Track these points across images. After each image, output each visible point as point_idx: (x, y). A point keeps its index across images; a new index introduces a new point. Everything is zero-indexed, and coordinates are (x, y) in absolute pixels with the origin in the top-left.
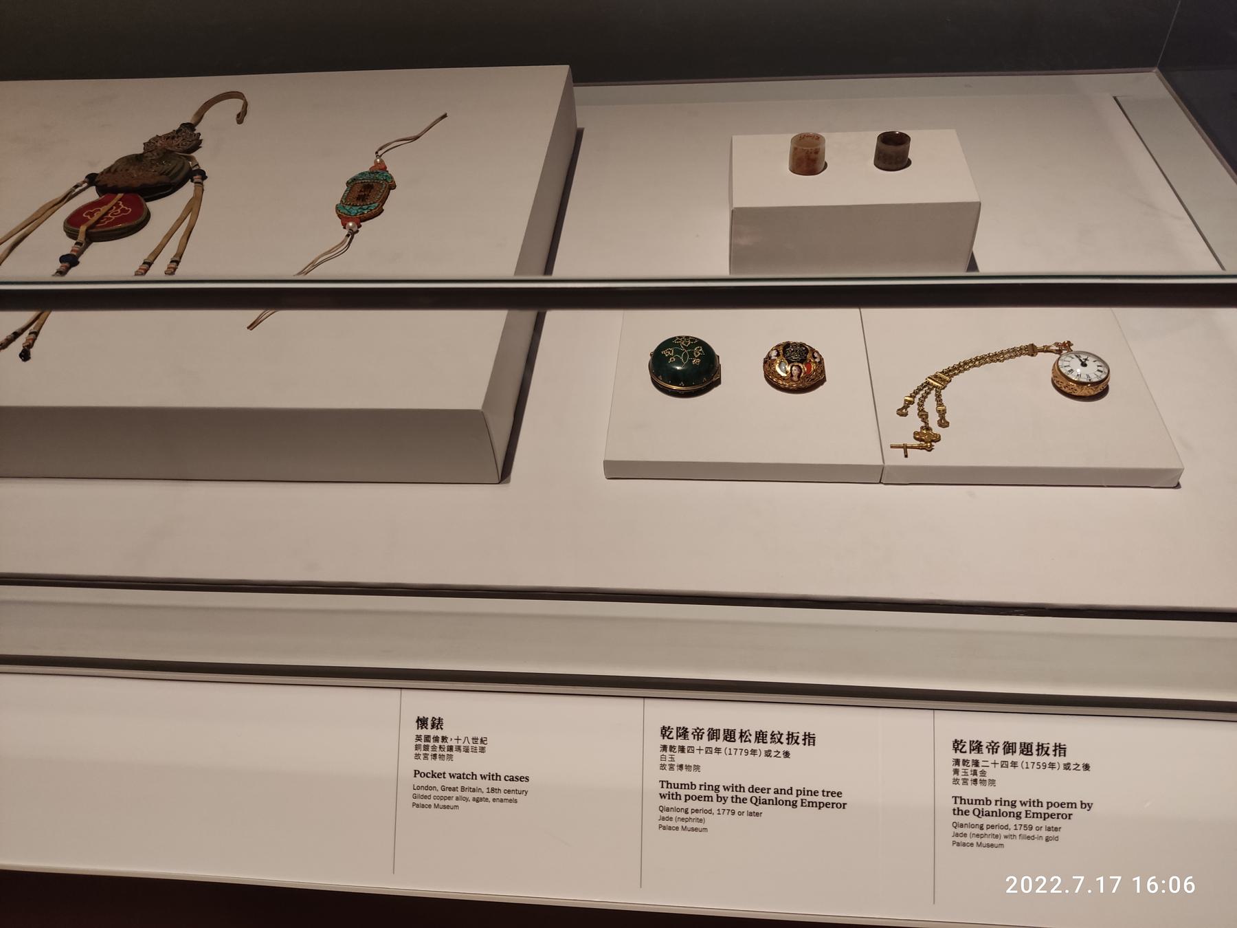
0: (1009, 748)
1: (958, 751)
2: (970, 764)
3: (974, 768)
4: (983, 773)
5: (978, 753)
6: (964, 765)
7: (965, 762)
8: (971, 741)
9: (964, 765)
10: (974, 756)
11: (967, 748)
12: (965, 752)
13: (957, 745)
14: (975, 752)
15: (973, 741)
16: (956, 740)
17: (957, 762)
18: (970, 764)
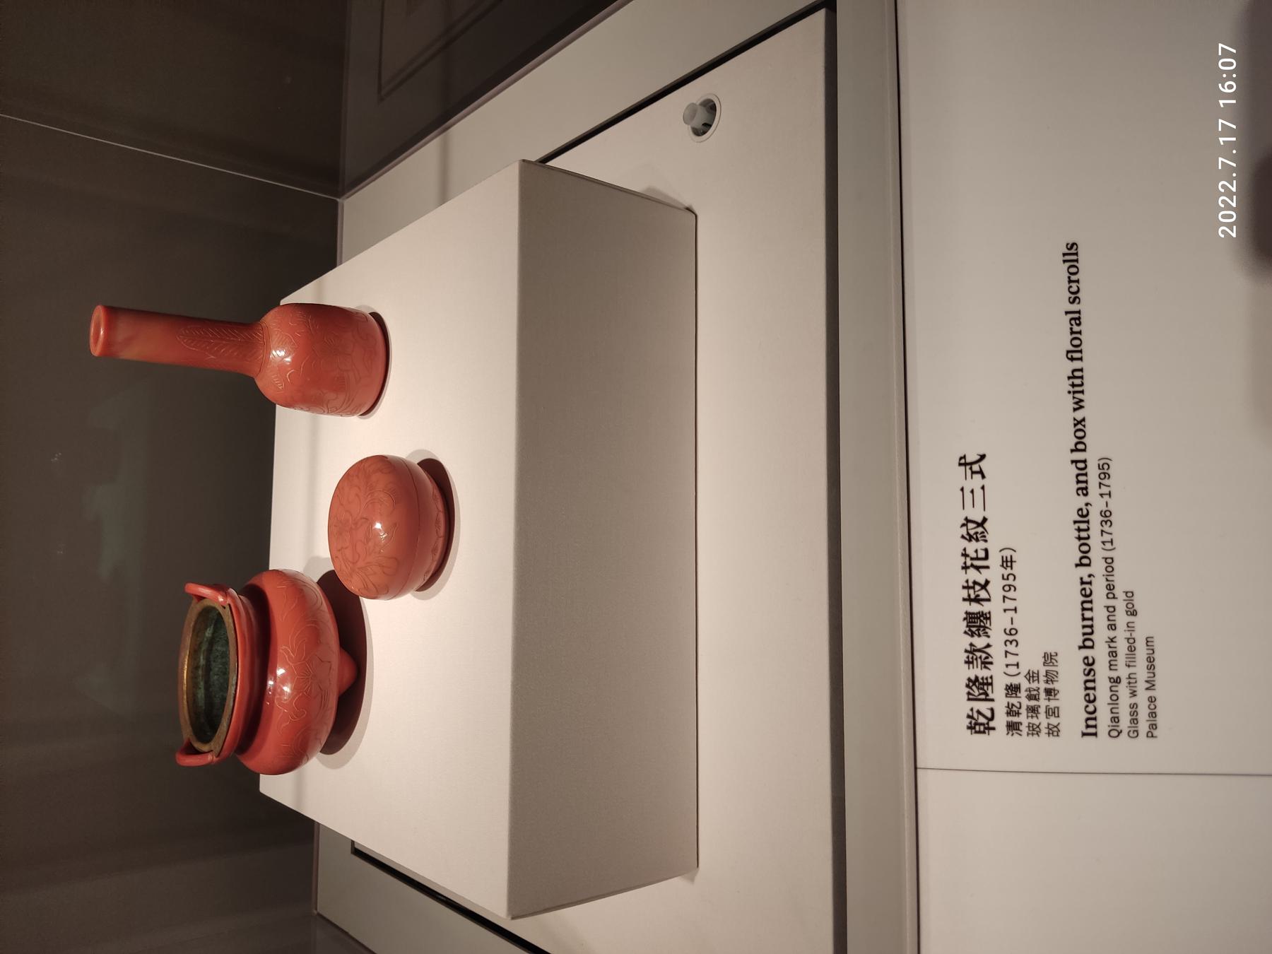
0: (977, 623)
1: (992, 724)
2: (1014, 701)
3: (1023, 694)
4: (1032, 676)
5: (991, 684)
6: (1018, 714)
7: (1011, 711)
8: (969, 699)
9: (1018, 714)
10: (998, 692)
11: (984, 707)
12: (992, 710)
13: (980, 725)
14: (989, 692)
15: (969, 693)
16: (969, 728)
17: (1013, 727)
18: (1014, 701)
